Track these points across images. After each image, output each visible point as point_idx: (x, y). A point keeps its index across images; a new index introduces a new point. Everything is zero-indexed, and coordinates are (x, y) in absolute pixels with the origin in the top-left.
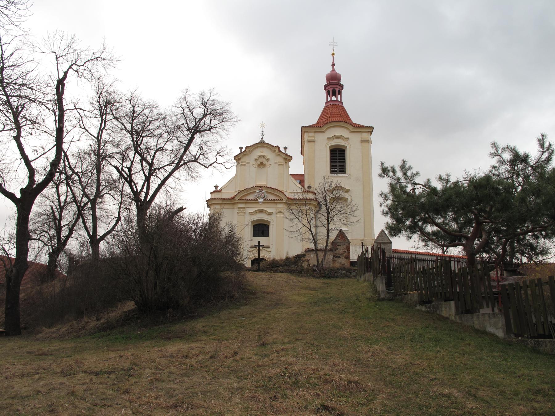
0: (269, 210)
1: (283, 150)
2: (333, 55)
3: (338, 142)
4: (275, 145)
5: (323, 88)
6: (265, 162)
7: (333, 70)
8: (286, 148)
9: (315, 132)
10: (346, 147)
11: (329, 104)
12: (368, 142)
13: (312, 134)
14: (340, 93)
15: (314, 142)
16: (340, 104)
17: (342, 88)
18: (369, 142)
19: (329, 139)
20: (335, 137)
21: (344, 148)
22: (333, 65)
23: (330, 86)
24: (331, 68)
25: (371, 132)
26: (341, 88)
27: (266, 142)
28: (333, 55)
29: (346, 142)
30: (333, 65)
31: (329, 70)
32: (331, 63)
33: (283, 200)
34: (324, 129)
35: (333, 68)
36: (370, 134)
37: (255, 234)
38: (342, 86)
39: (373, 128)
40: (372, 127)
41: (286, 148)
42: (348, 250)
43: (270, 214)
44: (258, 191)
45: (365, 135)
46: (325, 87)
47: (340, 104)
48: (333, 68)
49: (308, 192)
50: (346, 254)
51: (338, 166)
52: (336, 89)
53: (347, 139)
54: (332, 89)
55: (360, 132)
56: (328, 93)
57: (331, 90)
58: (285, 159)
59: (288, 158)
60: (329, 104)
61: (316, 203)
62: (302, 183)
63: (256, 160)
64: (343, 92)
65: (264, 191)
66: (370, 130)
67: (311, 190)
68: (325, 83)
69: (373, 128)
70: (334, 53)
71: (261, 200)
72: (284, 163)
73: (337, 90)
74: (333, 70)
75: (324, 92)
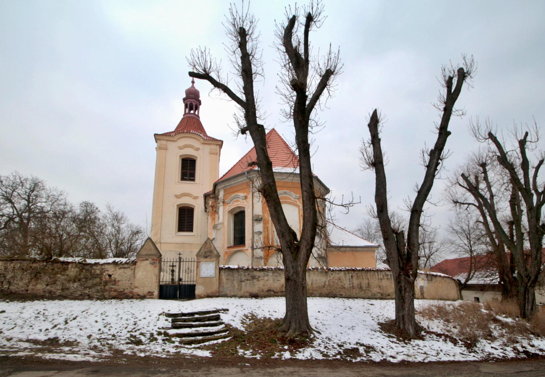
3: (189, 152)
7: (193, 86)
9: (167, 140)
10: (197, 157)
12: (216, 154)
13: (164, 142)
14: (197, 108)
15: (166, 150)
16: (196, 117)
17: (200, 104)
19: (180, 148)
20: (187, 146)
21: (195, 158)
24: (191, 85)
26: (198, 103)
29: (196, 152)
35: (193, 84)
36: (218, 147)
40: (220, 141)
45: (213, 147)
46: (184, 100)
47: (196, 117)
48: (193, 84)
51: (188, 174)
52: (193, 103)
54: (189, 102)
55: (210, 144)
56: (186, 106)
57: (188, 103)
66: (220, 144)
68: (184, 96)
73: (194, 104)
74: (193, 86)
75: (183, 105)
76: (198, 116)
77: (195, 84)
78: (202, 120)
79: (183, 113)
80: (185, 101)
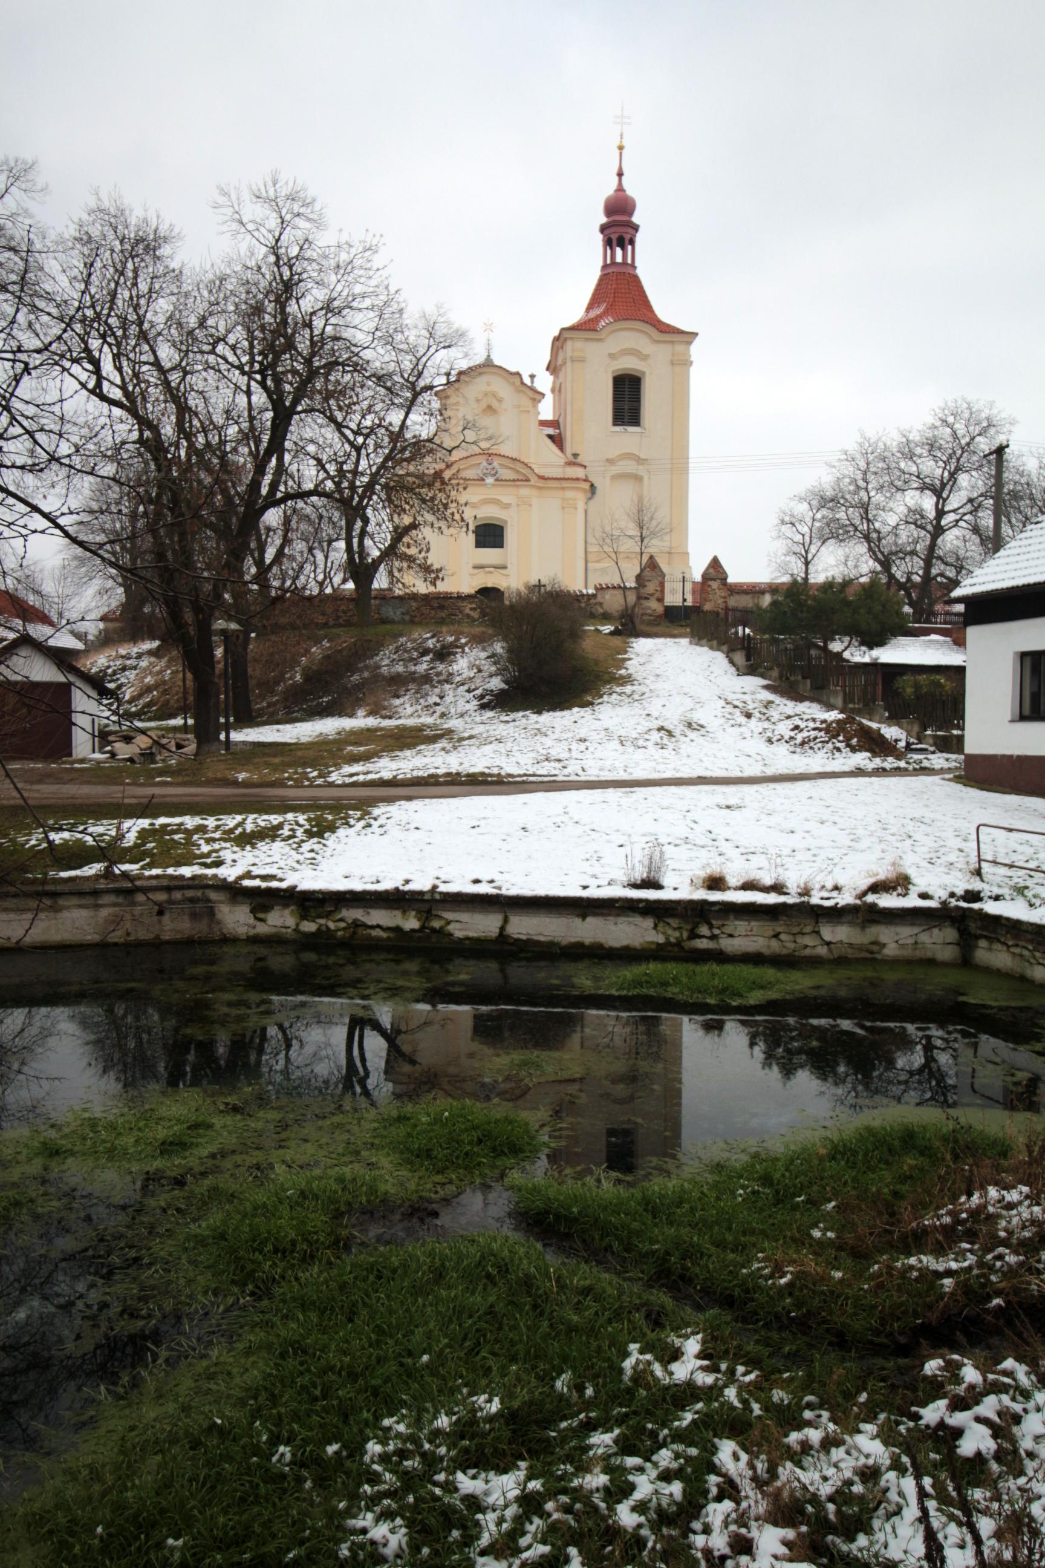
0: (505, 500)
1: (527, 381)
2: (621, 148)
3: (629, 364)
4: (513, 369)
5: (598, 228)
6: (495, 404)
7: (620, 189)
8: (532, 377)
9: (587, 339)
10: (644, 373)
11: (610, 270)
13: (579, 345)
18: (687, 363)
19: (612, 356)
22: (620, 174)
23: (612, 230)
25: (690, 343)
27: (496, 363)
28: (621, 148)
30: (620, 174)
31: (610, 190)
32: (616, 170)
33: (528, 480)
34: (603, 335)
37: (479, 544)
38: (636, 228)
39: (696, 334)
41: (532, 377)
42: (662, 585)
43: (507, 506)
44: (485, 463)
45: (679, 348)
46: (603, 229)
49: (574, 464)
50: (658, 594)
53: (644, 357)
55: (672, 342)
56: (608, 243)
57: (614, 237)
58: (534, 400)
59: (537, 397)
60: (610, 270)
61: (587, 486)
62: (557, 440)
63: (478, 401)
64: (639, 238)
65: (495, 464)
66: (690, 336)
67: (579, 460)
69: (696, 334)
70: (624, 143)
71: (490, 480)
72: (531, 408)
73: (627, 237)
74: (620, 189)
76: (633, 266)
77: (624, 178)
78: (642, 272)
79: (601, 263)
80: (607, 232)
